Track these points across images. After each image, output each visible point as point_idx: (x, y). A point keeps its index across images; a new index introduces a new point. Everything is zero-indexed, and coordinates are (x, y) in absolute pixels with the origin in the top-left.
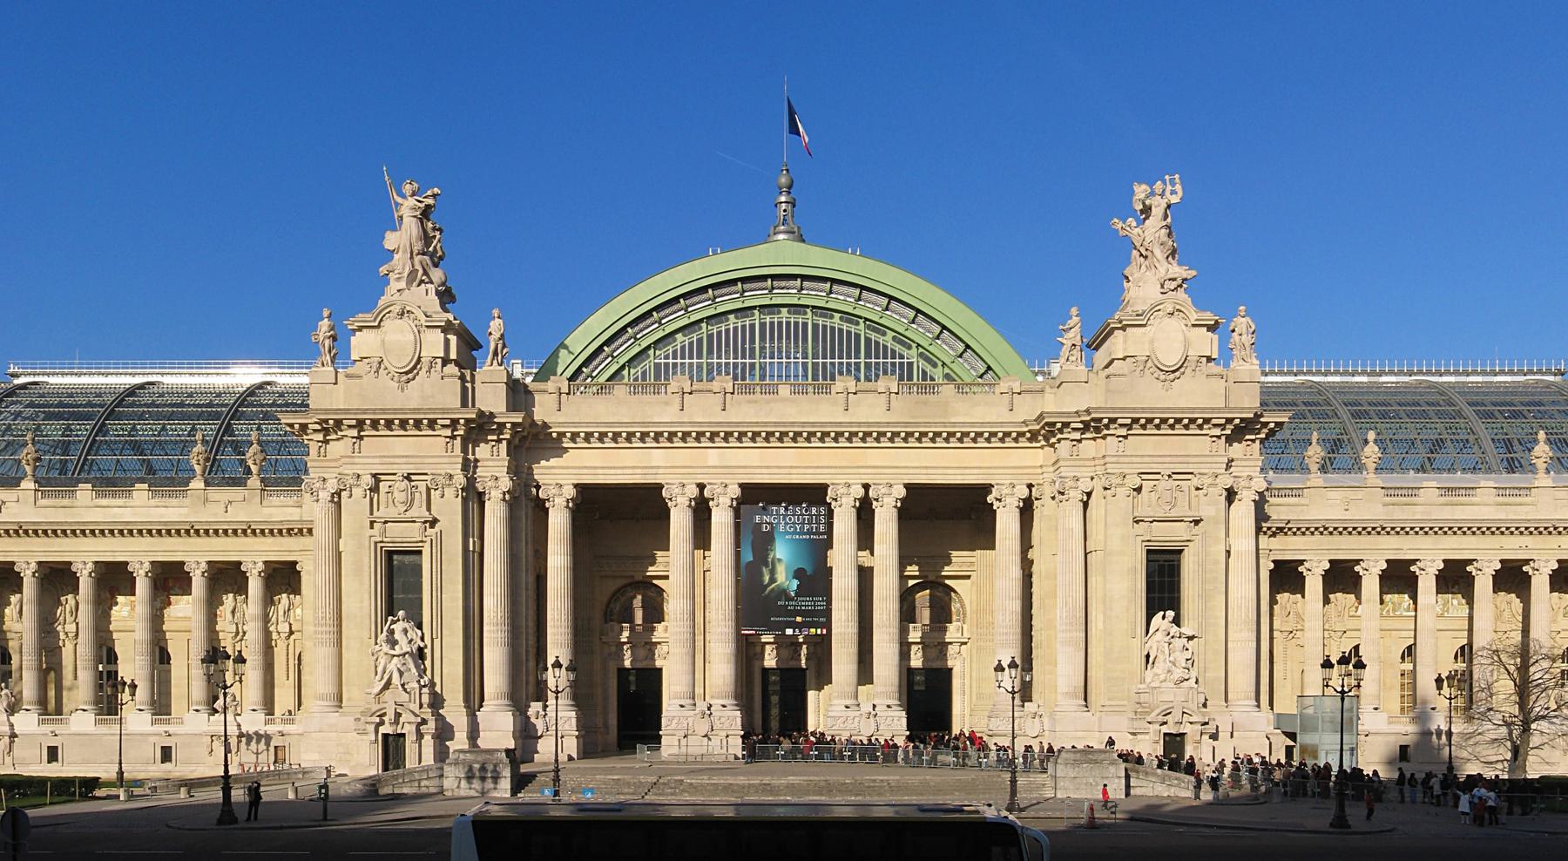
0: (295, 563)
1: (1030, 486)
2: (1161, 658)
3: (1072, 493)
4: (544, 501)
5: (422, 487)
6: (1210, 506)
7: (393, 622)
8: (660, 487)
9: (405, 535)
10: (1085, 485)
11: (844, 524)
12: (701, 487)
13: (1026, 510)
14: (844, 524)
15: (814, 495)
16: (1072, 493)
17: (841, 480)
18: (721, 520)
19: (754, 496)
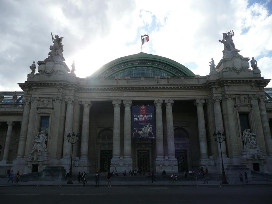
0: (20, 122)
1: (205, 100)
2: (248, 142)
3: (217, 100)
4: (83, 105)
5: (51, 100)
6: (254, 102)
7: (40, 134)
8: (112, 101)
9: (45, 112)
10: (221, 98)
11: (159, 110)
12: (122, 101)
13: (205, 106)
14: (159, 110)
15: (150, 104)
16: (217, 100)
17: (157, 99)
18: (128, 109)
19: (136, 104)
